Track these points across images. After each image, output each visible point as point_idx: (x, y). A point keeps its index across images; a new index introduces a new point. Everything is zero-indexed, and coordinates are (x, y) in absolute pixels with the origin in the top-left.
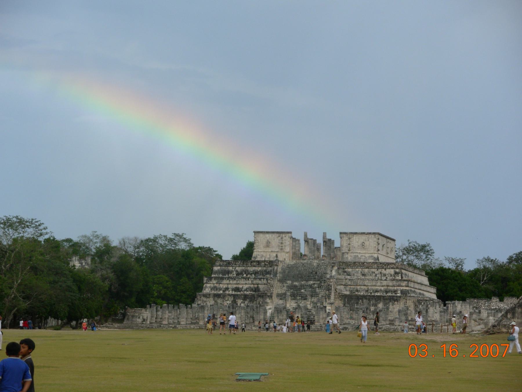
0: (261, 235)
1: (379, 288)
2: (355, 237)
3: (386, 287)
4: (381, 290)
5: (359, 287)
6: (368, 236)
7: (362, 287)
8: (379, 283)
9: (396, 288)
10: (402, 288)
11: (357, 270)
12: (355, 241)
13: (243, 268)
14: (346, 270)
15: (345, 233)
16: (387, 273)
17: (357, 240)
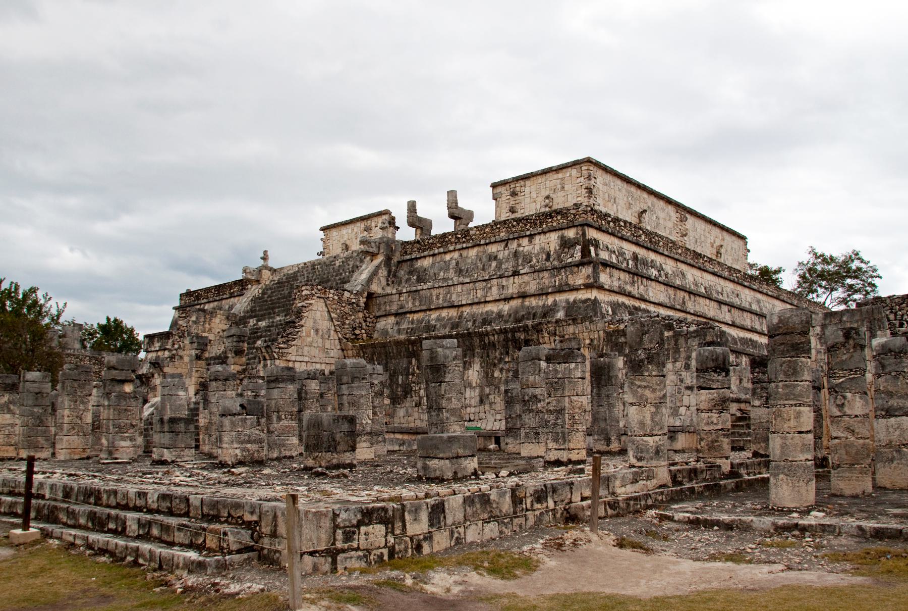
0: (334, 233)
1: (494, 308)
2: (527, 190)
3: (515, 303)
4: (500, 315)
5: (434, 315)
6: (560, 175)
7: (444, 313)
8: (495, 290)
9: (550, 300)
10: (571, 296)
11: (447, 257)
12: (527, 200)
13: (216, 303)
14: (419, 263)
15: (504, 183)
16: (537, 248)
17: (534, 195)
